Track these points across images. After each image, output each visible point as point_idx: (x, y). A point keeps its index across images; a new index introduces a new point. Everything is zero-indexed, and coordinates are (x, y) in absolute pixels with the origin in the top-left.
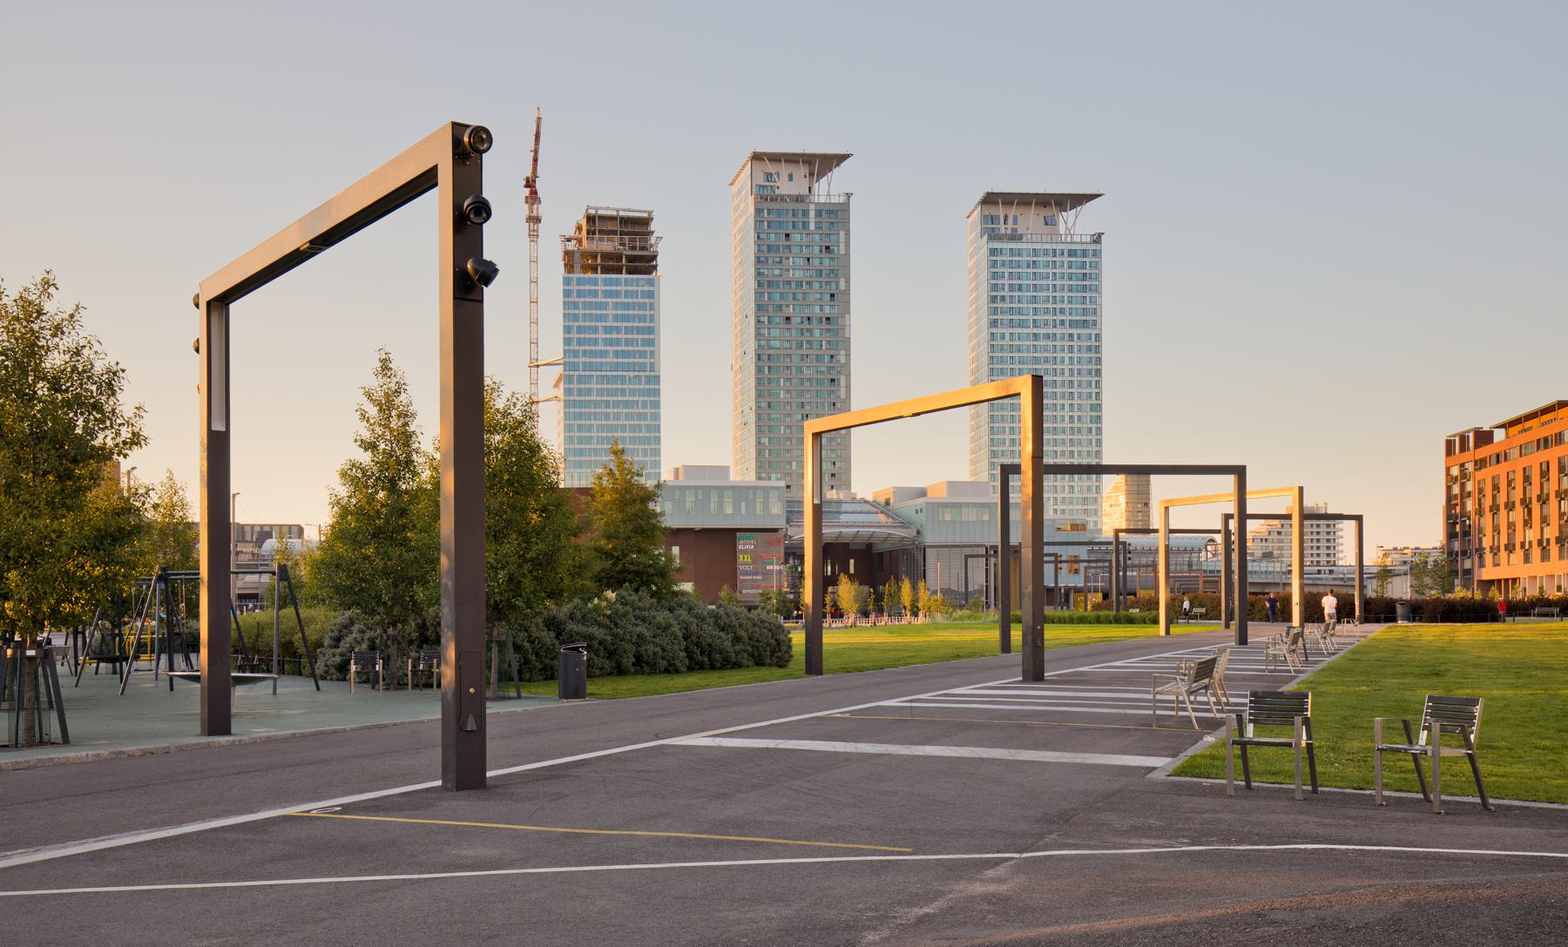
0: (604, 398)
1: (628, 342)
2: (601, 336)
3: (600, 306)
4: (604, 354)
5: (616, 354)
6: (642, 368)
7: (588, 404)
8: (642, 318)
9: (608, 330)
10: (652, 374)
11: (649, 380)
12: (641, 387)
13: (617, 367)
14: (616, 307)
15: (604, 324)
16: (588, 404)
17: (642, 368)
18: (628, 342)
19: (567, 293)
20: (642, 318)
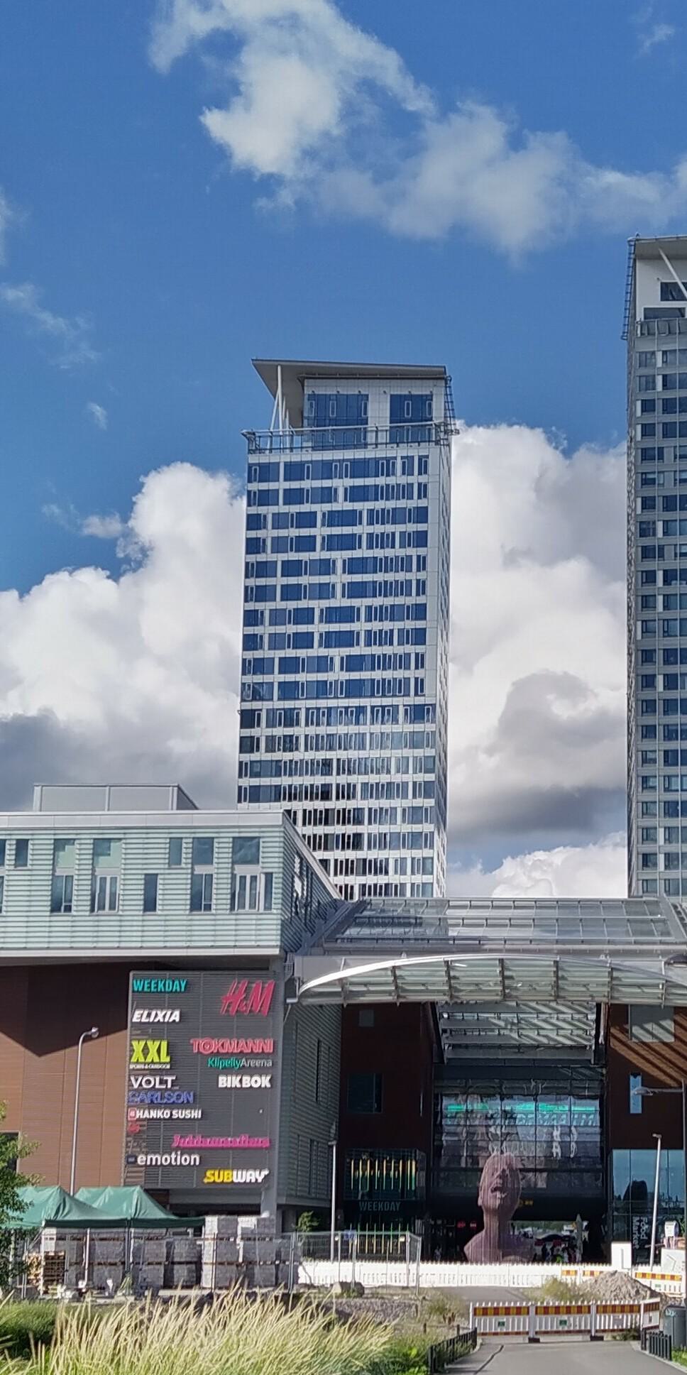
0: (321, 755)
1: (371, 638)
2: (318, 628)
3: (326, 567)
4: (323, 664)
5: (353, 663)
6: (400, 687)
7: (292, 768)
8: (404, 588)
9: (332, 615)
10: (419, 701)
11: (418, 713)
12: (397, 728)
13: (353, 689)
14: (353, 566)
15: (325, 604)
16: (292, 768)
17: (400, 687)
18: (371, 638)
19: (253, 546)
20: (404, 588)
